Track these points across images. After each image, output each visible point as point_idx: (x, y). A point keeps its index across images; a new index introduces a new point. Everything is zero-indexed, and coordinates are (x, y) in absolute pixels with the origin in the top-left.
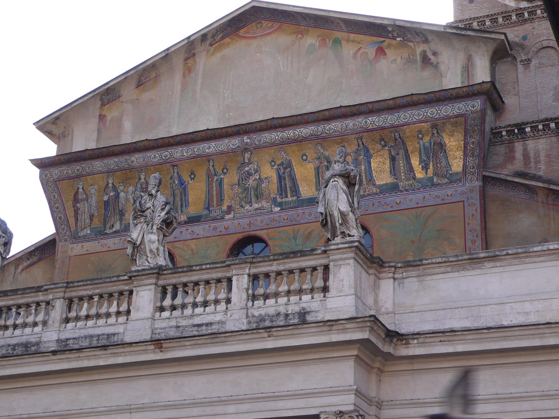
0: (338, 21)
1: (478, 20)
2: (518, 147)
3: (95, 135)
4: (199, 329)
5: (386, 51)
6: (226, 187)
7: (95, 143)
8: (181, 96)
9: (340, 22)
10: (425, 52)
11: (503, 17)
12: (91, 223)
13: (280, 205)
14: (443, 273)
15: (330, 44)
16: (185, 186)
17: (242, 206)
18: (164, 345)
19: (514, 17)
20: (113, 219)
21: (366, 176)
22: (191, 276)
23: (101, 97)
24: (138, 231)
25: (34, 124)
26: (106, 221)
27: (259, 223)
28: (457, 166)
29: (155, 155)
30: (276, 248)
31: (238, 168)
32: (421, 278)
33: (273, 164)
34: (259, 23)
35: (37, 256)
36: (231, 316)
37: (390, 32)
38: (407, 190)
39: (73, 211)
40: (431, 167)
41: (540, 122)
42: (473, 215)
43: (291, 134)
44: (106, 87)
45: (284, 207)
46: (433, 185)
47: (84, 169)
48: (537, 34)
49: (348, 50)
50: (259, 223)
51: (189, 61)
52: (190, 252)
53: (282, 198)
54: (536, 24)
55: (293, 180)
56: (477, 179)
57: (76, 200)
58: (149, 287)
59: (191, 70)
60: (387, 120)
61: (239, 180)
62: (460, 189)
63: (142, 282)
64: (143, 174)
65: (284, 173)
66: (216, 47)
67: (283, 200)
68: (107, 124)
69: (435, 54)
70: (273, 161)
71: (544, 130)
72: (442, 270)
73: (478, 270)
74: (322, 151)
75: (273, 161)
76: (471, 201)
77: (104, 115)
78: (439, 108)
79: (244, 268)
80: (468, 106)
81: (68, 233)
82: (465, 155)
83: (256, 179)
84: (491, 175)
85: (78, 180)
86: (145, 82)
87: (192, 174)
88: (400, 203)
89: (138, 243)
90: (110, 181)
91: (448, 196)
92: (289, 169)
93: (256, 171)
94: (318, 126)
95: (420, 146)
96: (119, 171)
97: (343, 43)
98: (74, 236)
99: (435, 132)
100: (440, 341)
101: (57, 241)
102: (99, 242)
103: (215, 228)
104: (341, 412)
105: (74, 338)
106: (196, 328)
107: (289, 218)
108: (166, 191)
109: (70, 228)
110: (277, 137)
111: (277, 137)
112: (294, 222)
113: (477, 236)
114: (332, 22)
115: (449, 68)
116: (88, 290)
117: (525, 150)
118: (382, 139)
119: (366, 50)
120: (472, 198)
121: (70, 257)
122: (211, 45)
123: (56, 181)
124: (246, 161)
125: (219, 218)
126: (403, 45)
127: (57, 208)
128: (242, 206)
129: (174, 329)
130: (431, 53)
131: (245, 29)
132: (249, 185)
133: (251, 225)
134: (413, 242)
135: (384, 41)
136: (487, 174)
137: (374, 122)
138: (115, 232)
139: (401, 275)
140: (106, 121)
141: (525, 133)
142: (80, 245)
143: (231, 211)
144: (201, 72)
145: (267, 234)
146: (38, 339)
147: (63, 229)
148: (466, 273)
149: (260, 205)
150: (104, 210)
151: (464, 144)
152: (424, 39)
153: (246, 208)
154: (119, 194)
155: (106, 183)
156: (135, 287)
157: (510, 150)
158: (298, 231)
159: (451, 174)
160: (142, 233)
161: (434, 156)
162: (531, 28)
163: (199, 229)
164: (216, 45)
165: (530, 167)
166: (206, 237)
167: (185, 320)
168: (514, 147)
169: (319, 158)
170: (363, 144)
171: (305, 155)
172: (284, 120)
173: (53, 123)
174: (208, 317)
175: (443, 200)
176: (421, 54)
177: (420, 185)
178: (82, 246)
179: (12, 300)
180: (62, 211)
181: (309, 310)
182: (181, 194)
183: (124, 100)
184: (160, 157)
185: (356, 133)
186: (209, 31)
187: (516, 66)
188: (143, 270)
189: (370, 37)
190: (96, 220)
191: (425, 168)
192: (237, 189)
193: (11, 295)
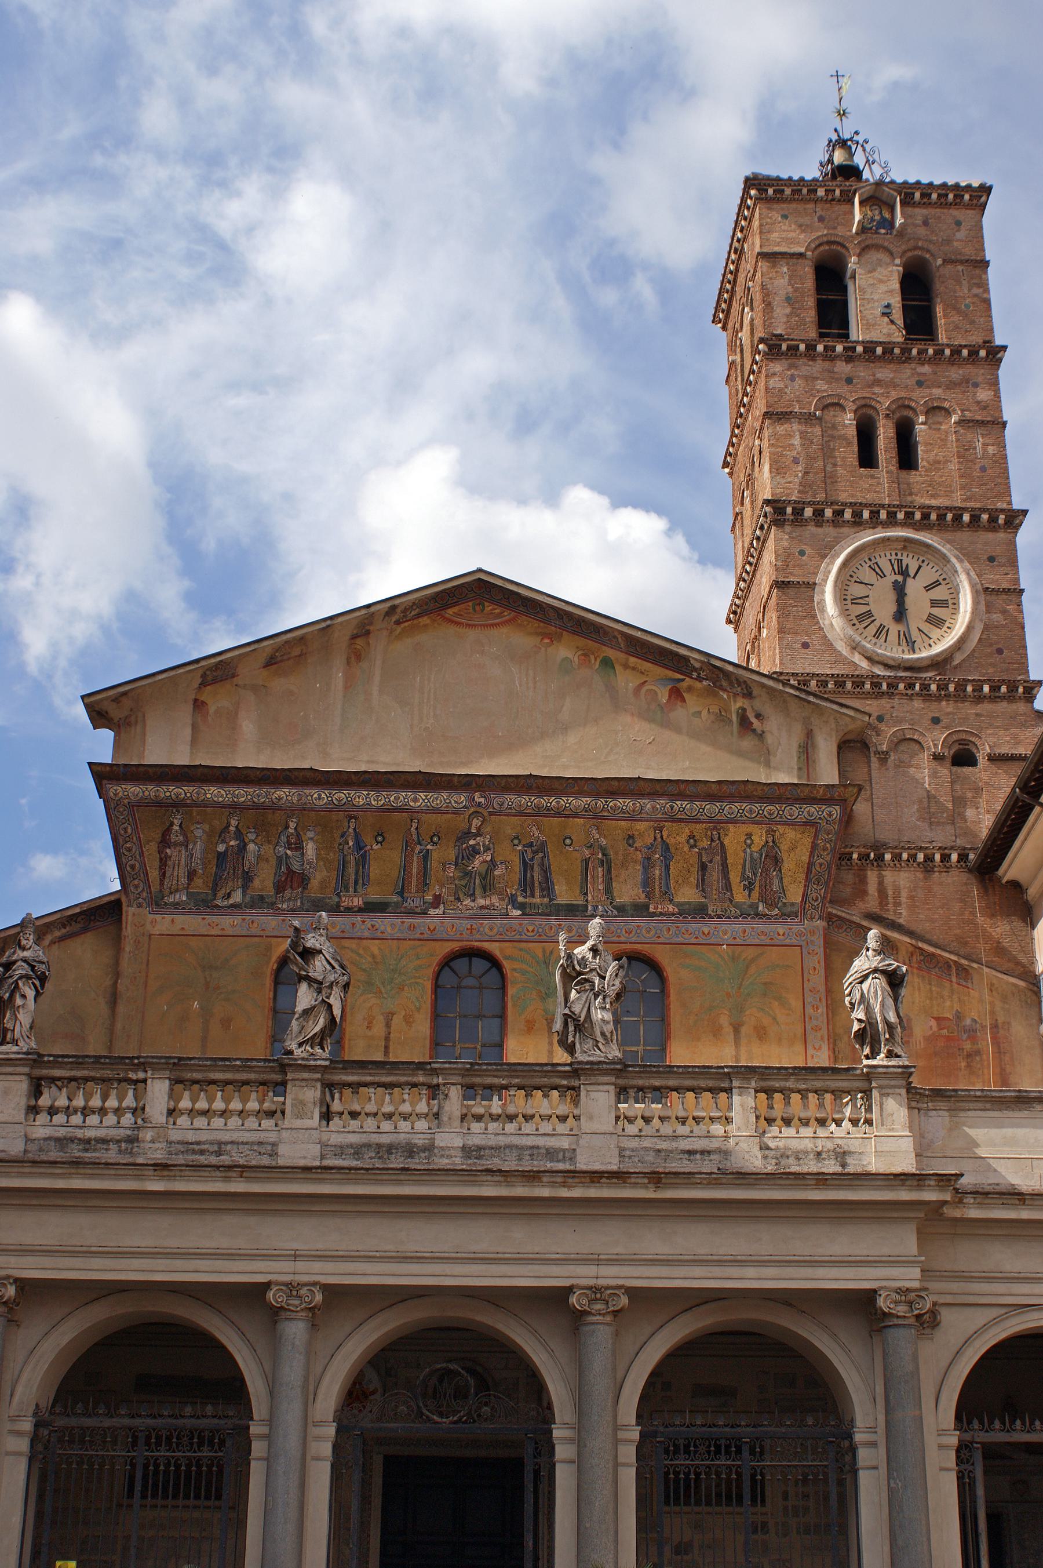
0: (616, 634)
1: (818, 678)
2: (872, 876)
3: (188, 731)
4: (692, 1157)
5: (685, 695)
6: (434, 864)
7: (188, 747)
8: (344, 697)
9: (619, 636)
10: (744, 710)
11: (853, 683)
12: (189, 884)
13: (521, 906)
14: (981, 1110)
15: (597, 666)
16: (366, 852)
17: (458, 899)
18: (664, 1181)
19: (868, 686)
20: (230, 884)
21: (661, 888)
22: (667, 1078)
23: (205, 673)
24: (583, 1002)
25: (83, 697)
26: (217, 885)
27: (486, 930)
28: (794, 895)
29: (320, 795)
30: (516, 974)
31: (458, 839)
32: (953, 1113)
33: (516, 842)
34: (479, 604)
35: (79, 922)
36: (737, 1144)
37: (695, 669)
38: (719, 917)
39: (158, 860)
40: (757, 888)
41: (905, 849)
42: (815, 968)
43: (553, 803)
44: (219, 659)
45: (527, 911)
46: (757, 914)
47: (188, 795)
48: (897, 717)
49: (625, 681)
50: (486, 930)
51: (359, 641)
52: (370, 959)
53: (525, 897)
54: (896, 701)
55: (545, 872)
56: (820, 917)
57: (165, 842)
58: (606, 1087)
59: (360, 655)
60: (704, 809)
61: (457, 858)
62: (796, 928)
63: (593, 1079)
64: (295, 820)
65: (532, 859)
66: (405, 627)
67: (527, 900)
68: (210, 718)
69: (758, 716)
70: (517, 838)
71: (908, 860)
72: (980, 1105)
73: (1026, 1112)
74: (597, 836)
75: (517, 838)
76: (812, 948)
77: (203, 702)
78: (781, 807)
79: (748, 1079)
80: (823, 812)
81: (145, 894)
82: (808, 879)
83: (485, 862)
84: (839, 913)
85: (174, 811)
86: (281, 661)
87: (379, 835)
88: (708, 934)
89: (582, 1019)
90: (234, 823)
91: (779, 935)
92: (541, 855)
93: (487, 849)
94: (597, 798)
95: (745, 856)
96: (253, 809)
97: (618, 668)
98: (156, 902)
99: (770, 840)
100: (1003, 1204)
101: (124, 905)
102: (204, 919)
103: (412, 928)
104: (907, 1289)
105: (493, 1148)
106: (686, 1156)
107: (536, 929)
108: (331, 854)
109: (150, 887)
110: (529, 804)
111: (529, 804)
112: (545, 937)
113: (820, 1000)
114: (606, 633)
115: (780, 743)
116: (500, 1077)
117: (881, 883)
118: (692, 836)
119: (654, 688)
120: (812, 941)
121: (150, 935)
122: (398, 623)
123: (133, 806)
124: (473, 830)
125: (419, 911)
126: (711, 693)
127: (129, 850)
128: (458, 899)
129: (652, 1153)
130: (753, 714)
131: (455, 609)
132: (473, 868)
133: (474, 931)
134: (728, 995)
135: (684, 680)
136: (834, 912)
137: (684, 809)
138: (232, 906)
139: (926, 1105)
140: (208, 713)
141: (883, 860)
142: (168, 918)
143: (439, 904)
144: (378, 663)
145: (501, 950)
146: (427, 1141)
147: (136, 887)
148: (1010, 1114)
149: (488, 903)
150: (217, 866)
151: (808, 864)
152: (745, 691)
153: (464, 903)
154: (245, 845)
155: (225, 825)
156: (583, 1084)
157: (860, 880)
158: (551, 952)
159: (785, 904)
160: (587, 1005)
161: (764, 875)
162: (888, 706)
163: (385, 924)
164: (406, 624)
165: (888, 910)
166: (398, 939)
167: (665, 1141)
168: (865, 877)
169: (591, 846)
170: (662, 837)
171: (570, 838)
172: (547, 781)
173: (113, 701)
174: (700, 1142)
175: (772, 939)
176: (738, 712)
177: (738, 912)
178: (173, 921)
179: (370, 1075)
180: (138, 857)
181: (846, 1148)
182: (357, 864)
183: (240, 683)
184: (330, 799)
185: (657, 821)
186: (402, 603)
187: (869, 757)
188: (600, 1062)
189: (663, 669)
190: (198, 882)
191: (749, 888)
192: (451, 870)
193: (371, 1069)
